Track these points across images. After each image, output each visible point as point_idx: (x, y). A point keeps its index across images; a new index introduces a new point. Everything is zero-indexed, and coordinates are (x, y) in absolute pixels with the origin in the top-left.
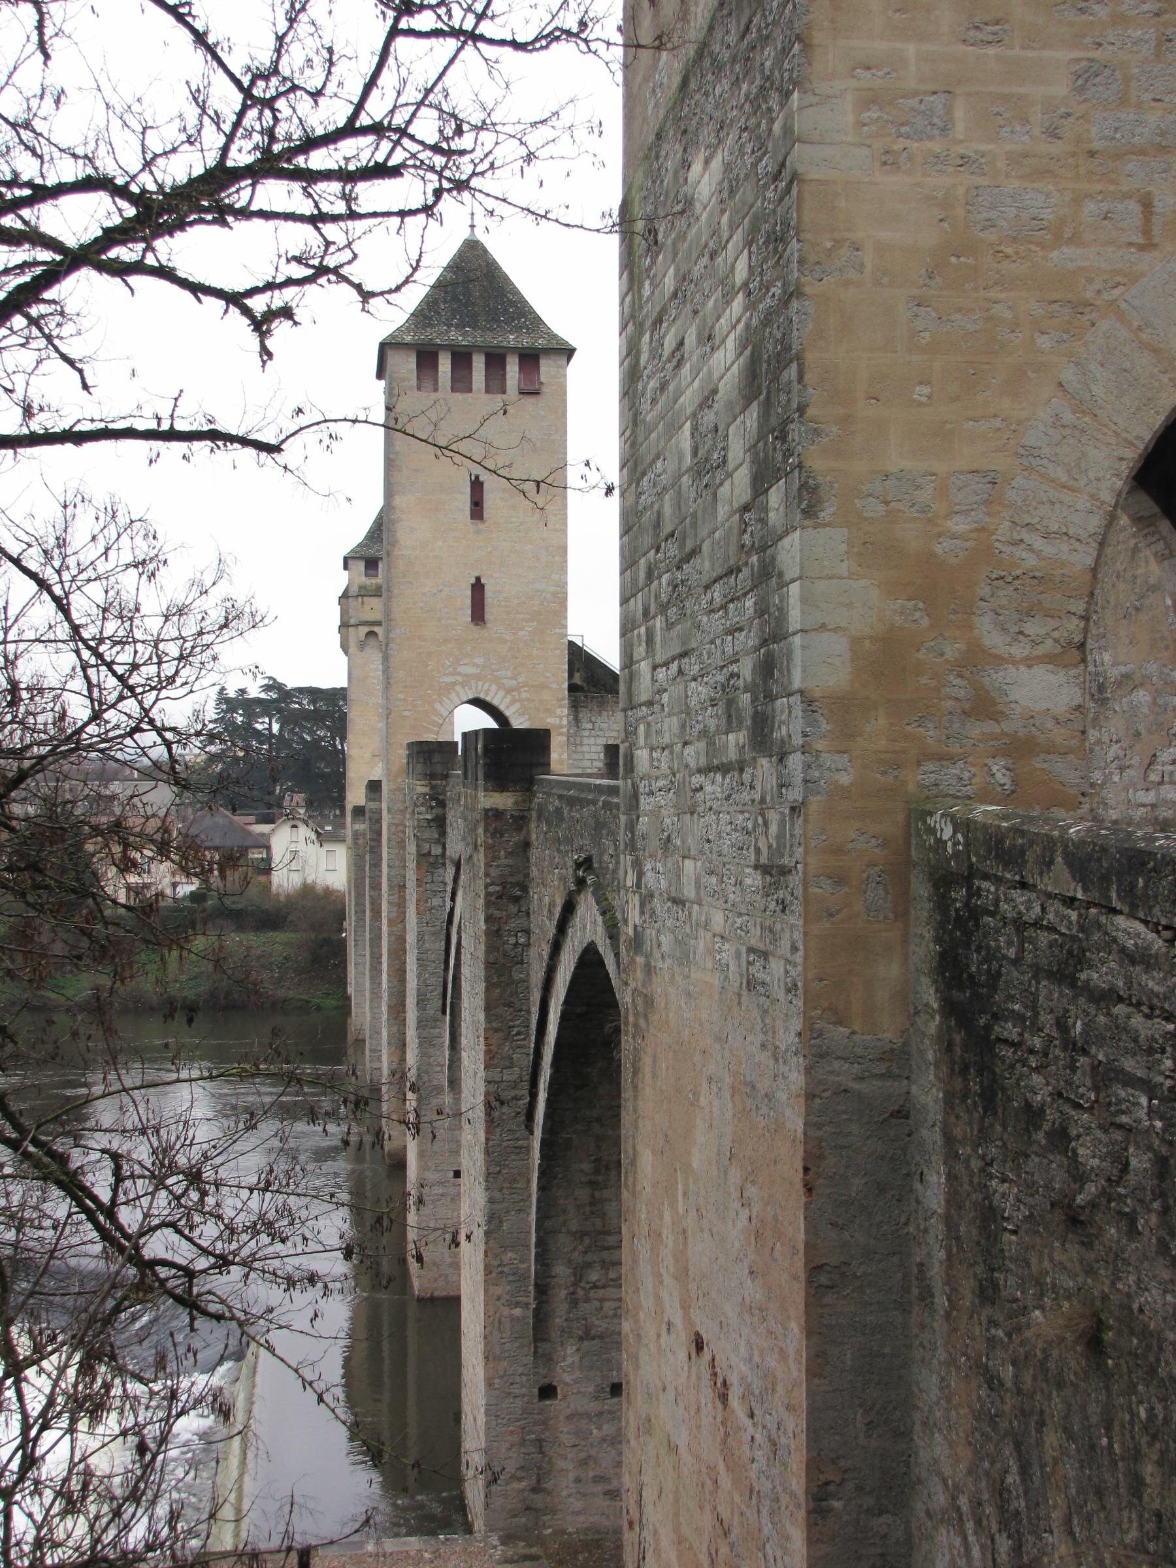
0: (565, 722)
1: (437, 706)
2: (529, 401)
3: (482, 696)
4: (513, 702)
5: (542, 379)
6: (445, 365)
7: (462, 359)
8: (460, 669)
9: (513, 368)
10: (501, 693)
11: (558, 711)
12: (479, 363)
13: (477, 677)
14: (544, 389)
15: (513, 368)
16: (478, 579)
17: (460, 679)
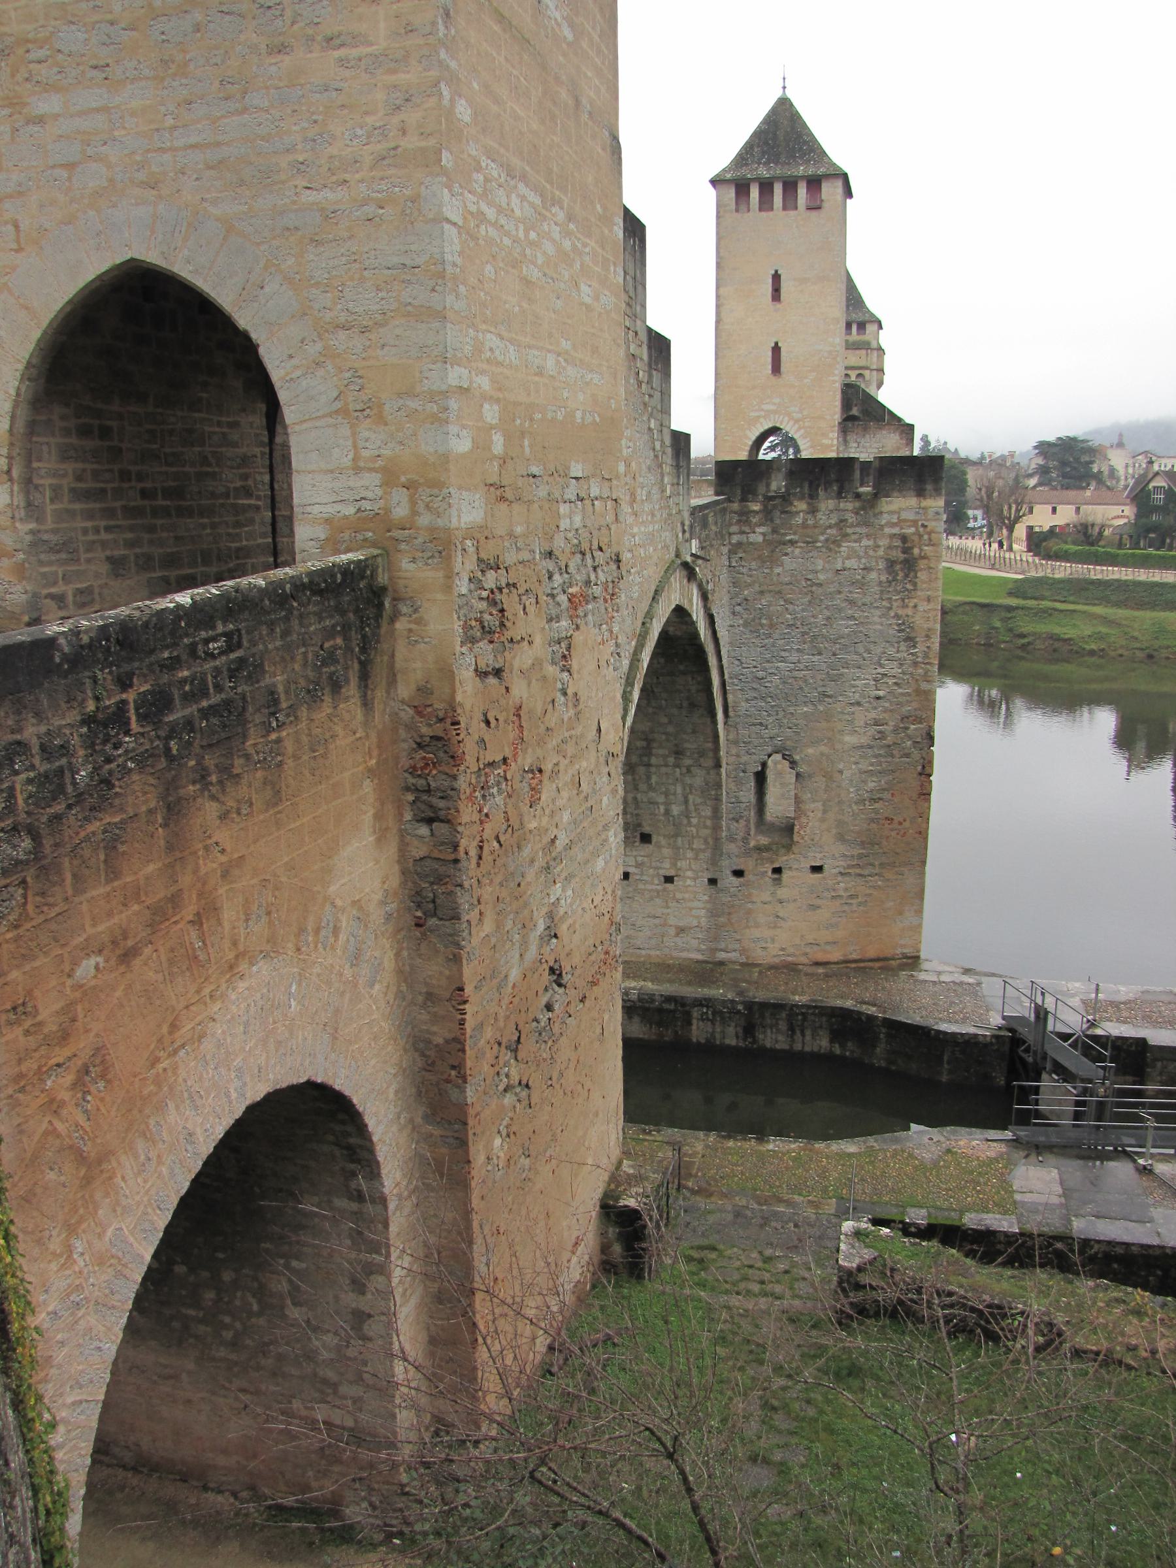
0: (835, 442)
1: (748, 432)
2: (814, 214)
3: (778, 425)
4: (799, 429)
5: (823, 197)
6: (755, 192)
7: (766, 187)
8: (764, 407)
9: (802, 191)
10: (791, 423)
11: (831, 435)
12: (778, 189)
13: (775, 412)
14: (825, 205)
15: (802, 191)
16: (776, 344)
17: (763, 413)
